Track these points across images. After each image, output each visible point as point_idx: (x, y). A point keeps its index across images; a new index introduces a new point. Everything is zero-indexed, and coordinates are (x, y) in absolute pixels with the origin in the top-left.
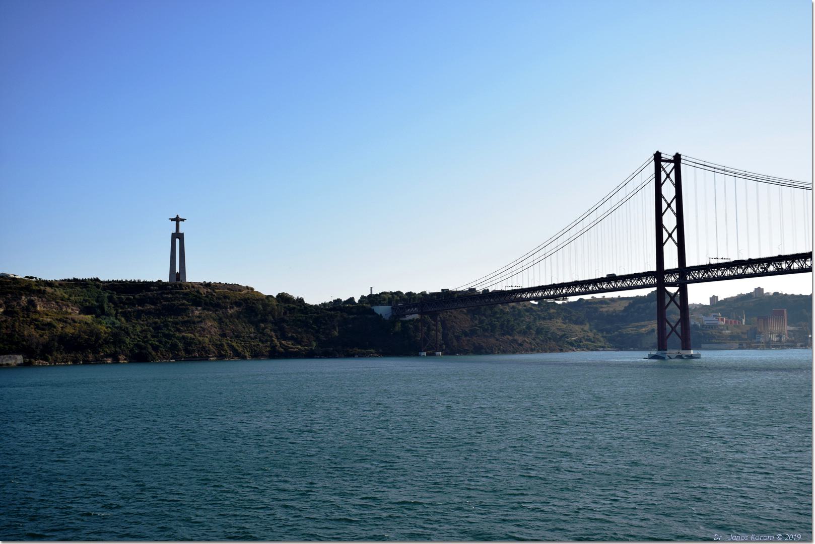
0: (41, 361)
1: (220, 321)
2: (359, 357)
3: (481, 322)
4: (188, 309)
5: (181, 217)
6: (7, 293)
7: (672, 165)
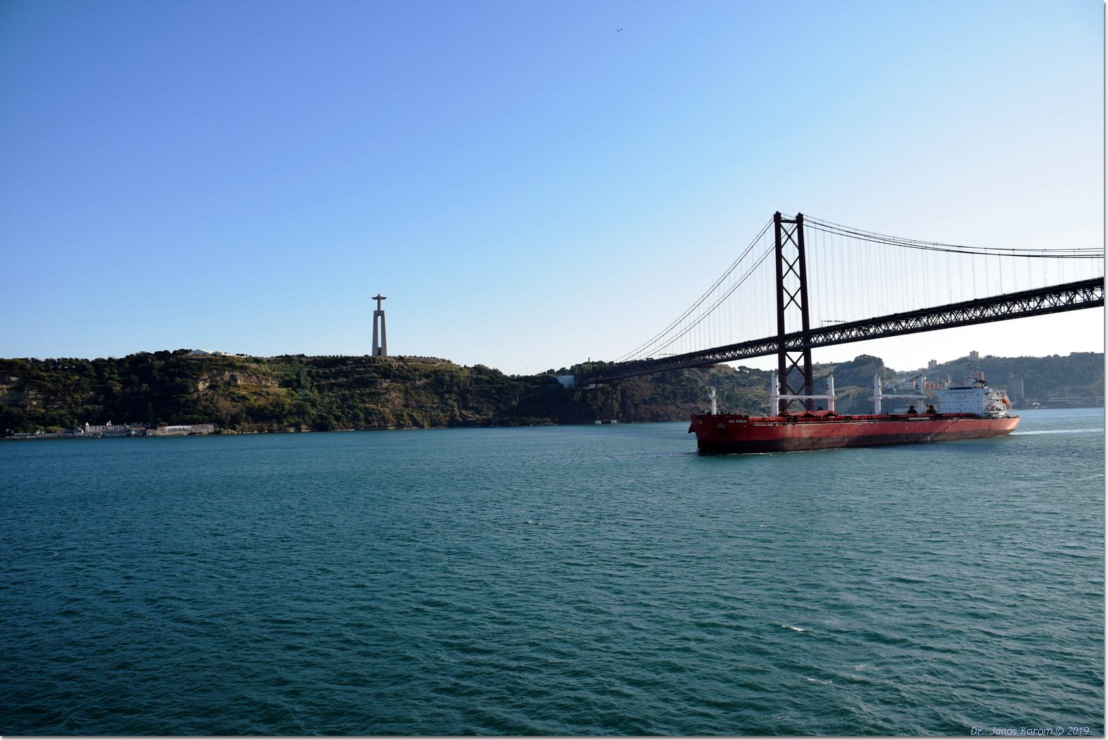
0: (230, 430)
1: (406, 392)
2: (534, 425)
3: (664, 390)
4: (376, 381)
5: (381, 296)
6: (212, 370)
7: (796, 225)
